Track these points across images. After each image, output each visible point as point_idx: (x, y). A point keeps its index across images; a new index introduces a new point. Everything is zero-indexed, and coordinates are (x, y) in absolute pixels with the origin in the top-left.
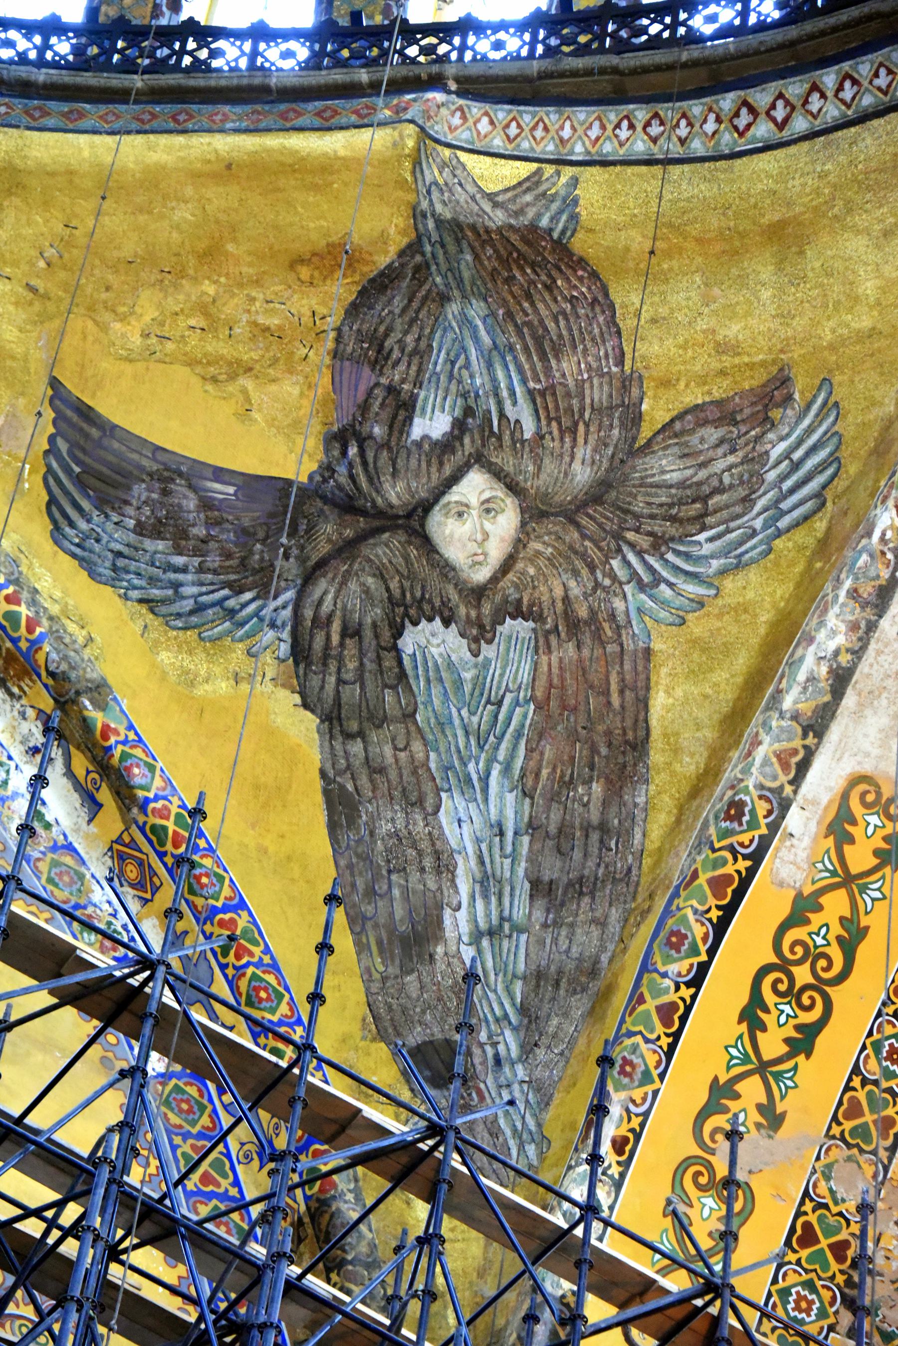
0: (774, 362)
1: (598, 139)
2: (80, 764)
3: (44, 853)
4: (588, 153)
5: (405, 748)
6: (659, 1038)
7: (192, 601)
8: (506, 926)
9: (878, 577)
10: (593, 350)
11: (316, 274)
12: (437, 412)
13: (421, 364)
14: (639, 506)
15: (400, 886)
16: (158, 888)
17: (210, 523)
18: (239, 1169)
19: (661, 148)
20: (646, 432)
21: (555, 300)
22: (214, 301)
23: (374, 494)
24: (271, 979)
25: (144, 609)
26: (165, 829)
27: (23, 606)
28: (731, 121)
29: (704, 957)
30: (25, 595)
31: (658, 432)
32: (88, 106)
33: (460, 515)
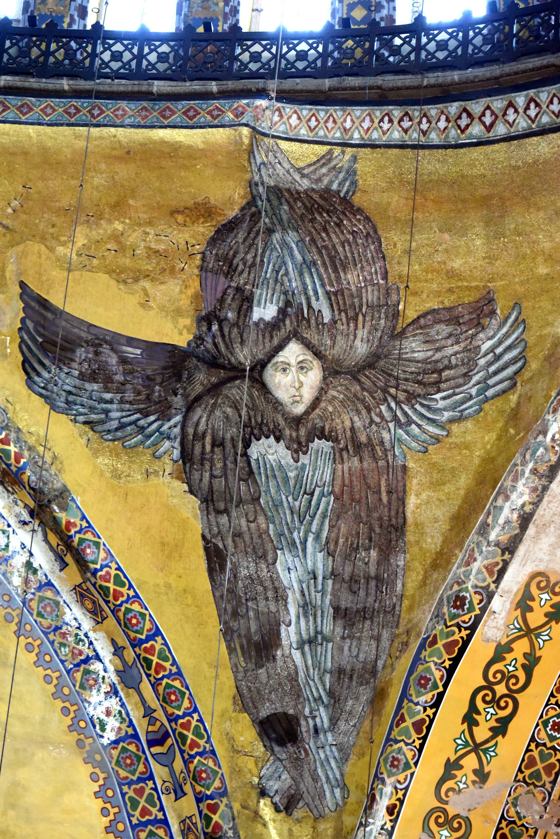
0: (485, 287)
1: (368, 129)
2: (53, 539)
3: (33, 594)
4: (363, 139)
5: (254, 521)
6: (414, 741)
7: (117, 422)
8: (319, 637)
9: (550, 460)
10: (368, 268)
11: (188, 219)
12: (268, 304)
15: (254, 609)
18: (163, 797)
19: (410, 137)
21: (342, 232)
22: (122, 234)
23: (230, 356)
25: (87, 428)
26: (108, 588)
27: (12, 444)
28: (456, 121)
29: (441, 689)
30: (13, 436)
31: (409, 325)
32: (33, 99)
33: (284, 370)
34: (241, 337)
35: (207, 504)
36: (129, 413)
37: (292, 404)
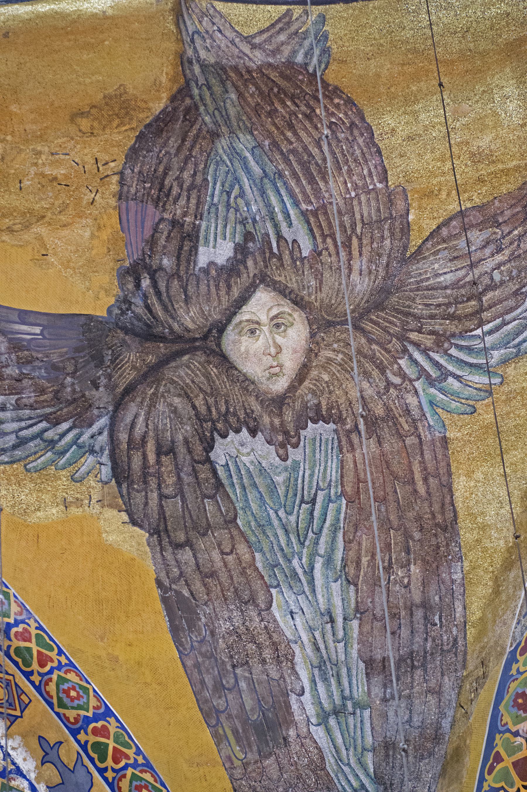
5: (232, 552)
7: (13, 436)
8: (349, 704)
10: (358, 170)
11: (96, 124)
12: (219, 240)
13: (199, 197)
14: (418, 309)
15: (245, 677)
16: (27, 705)
17: (21, 363)
20: (415, 241)
23: (170, 321)
24: (147, 776)
26: (29, 650)
31: (427, 240)
33: (252, 332)
34: (185, 292)
35: (159, 536)
36: (30, 422)
37: (268, 379)
